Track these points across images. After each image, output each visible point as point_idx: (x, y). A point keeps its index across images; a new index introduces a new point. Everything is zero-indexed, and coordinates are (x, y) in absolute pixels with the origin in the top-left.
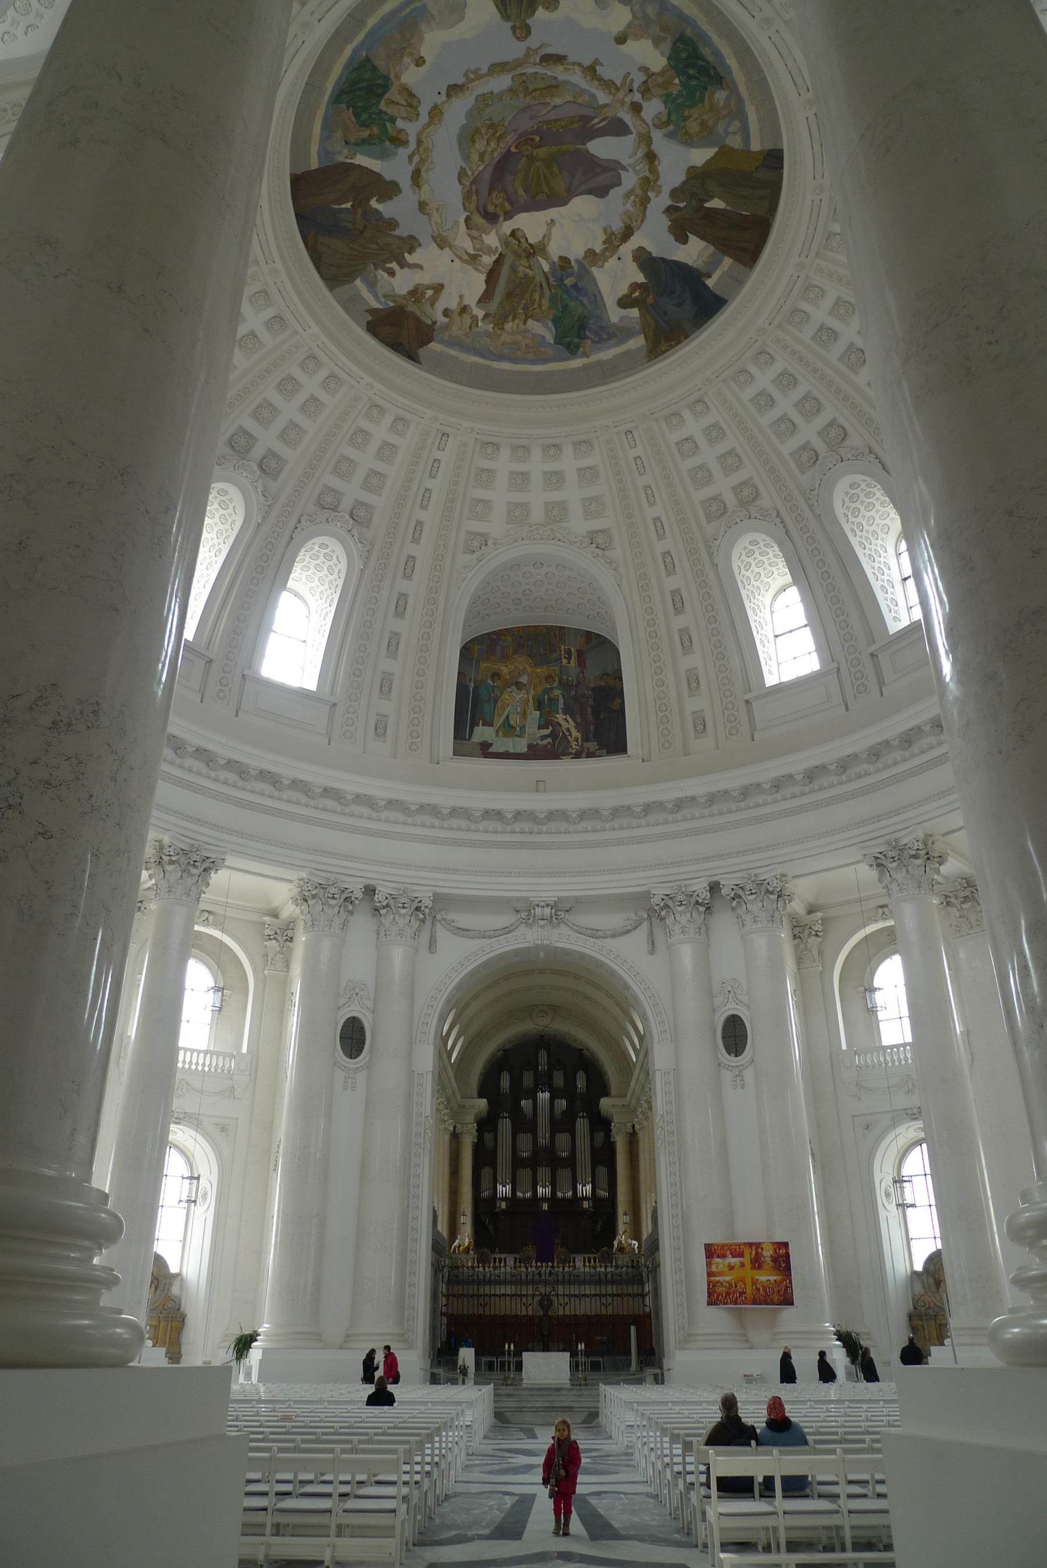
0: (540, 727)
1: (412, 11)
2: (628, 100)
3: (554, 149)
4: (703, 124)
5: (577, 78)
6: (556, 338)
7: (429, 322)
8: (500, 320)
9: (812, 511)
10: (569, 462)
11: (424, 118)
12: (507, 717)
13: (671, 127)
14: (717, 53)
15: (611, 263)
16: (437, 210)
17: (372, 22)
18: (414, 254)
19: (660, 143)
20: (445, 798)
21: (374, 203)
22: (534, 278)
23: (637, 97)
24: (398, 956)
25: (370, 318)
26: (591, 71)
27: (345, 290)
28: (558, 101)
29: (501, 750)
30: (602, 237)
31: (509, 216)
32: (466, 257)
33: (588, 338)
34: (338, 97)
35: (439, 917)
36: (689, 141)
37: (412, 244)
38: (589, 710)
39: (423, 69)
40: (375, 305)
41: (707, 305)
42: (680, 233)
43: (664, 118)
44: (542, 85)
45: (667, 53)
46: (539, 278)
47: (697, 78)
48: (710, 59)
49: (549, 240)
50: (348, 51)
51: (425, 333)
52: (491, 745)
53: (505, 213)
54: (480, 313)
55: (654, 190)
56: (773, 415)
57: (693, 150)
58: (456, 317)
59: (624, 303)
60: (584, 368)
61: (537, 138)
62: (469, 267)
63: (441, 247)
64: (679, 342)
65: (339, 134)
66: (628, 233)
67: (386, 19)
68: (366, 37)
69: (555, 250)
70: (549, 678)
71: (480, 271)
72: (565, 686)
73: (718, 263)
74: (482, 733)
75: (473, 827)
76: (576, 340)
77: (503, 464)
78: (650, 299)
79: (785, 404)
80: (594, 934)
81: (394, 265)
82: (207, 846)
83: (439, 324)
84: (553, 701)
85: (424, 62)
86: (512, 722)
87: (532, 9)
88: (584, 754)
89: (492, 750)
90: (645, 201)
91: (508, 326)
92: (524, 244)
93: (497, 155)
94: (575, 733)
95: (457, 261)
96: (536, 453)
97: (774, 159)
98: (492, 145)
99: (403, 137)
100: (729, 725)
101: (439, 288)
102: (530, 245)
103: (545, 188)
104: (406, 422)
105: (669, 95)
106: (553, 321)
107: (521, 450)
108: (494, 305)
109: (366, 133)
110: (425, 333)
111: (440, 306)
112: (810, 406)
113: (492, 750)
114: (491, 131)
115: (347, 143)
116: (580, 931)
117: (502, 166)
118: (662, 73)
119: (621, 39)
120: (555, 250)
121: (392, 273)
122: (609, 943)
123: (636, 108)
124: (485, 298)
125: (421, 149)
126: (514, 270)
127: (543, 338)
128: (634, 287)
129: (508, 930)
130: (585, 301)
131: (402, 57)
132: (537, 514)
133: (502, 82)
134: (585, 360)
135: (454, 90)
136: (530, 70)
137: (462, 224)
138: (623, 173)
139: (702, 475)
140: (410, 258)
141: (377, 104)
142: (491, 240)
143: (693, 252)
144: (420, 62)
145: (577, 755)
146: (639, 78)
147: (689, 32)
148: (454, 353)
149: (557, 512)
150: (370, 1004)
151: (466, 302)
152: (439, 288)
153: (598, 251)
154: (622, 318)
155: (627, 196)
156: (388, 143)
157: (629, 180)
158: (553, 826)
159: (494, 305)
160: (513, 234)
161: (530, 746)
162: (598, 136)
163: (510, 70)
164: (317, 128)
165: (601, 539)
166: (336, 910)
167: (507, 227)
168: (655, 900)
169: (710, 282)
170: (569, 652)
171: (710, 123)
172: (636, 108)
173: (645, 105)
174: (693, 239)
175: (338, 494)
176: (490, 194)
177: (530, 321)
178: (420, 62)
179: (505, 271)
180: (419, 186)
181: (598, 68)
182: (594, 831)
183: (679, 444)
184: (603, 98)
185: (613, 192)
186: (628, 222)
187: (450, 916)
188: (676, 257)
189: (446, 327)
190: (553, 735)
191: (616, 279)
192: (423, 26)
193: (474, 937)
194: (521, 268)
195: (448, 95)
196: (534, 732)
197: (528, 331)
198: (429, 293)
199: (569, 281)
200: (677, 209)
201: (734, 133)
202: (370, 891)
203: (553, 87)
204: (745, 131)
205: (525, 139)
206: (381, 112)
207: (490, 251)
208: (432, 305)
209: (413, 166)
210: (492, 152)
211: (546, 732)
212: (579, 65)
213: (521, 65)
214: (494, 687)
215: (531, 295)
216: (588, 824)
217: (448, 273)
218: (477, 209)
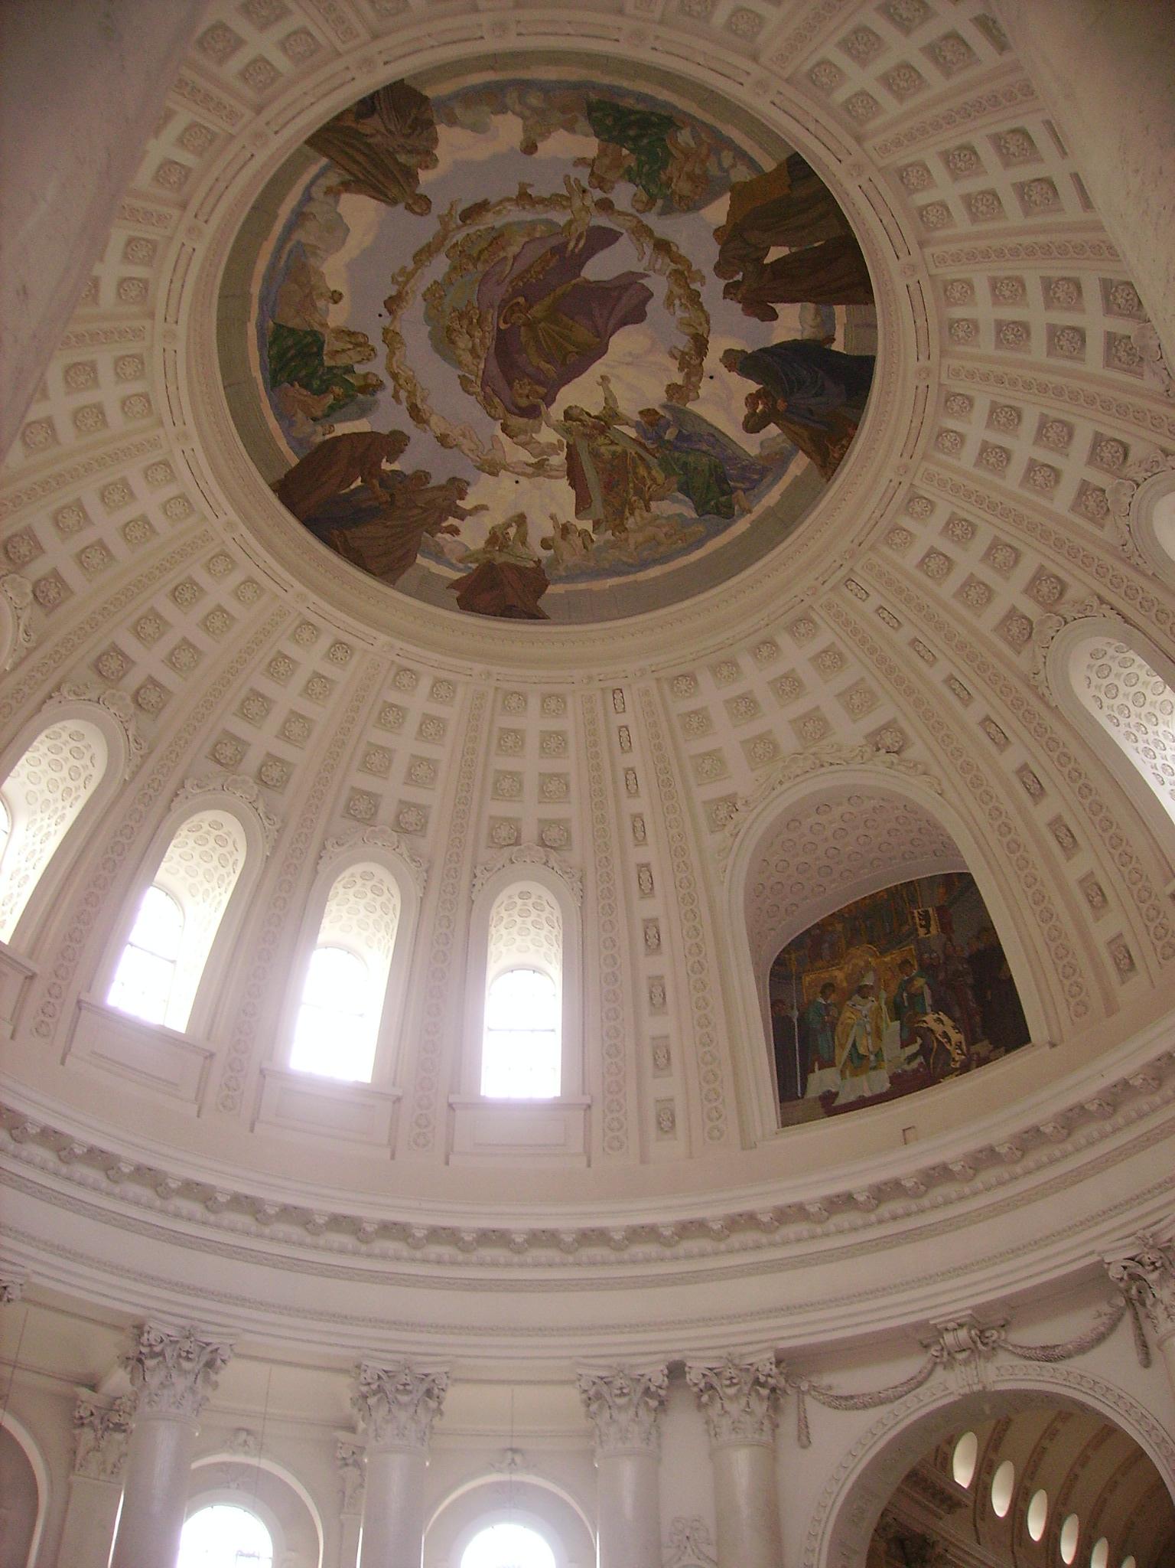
0: (903, 1045)
1: (291, 251)
2: (588, 202)
3: (548, 301)
4: (691, 177)
5: (516, 214)
7: (531, 564)
8: (616, 519)
9: (1144, 574)
10: (795, 656)
11: (382, 349)
12: (854, 1045)
13: (660, 203)
14: (641, 97)
15: (705, 388)
16: (464, 436)
17: (256, 289)
18: (467, 497)
20: (762, 1201)
21: (386, 466)
22: (625, 453)
23: (598, 194)
24: (742, 1463)
25: (457, 594)
27: (409, 576)
28: (514, 249)
29: (852, 1098)
30: (674, 365)
31: (550, 400)
32: (530, 470)
33: (736, 488)
34: (273, 382)
35: (805, 1386)
36: (691, 205)
37: (458, 487)
38: (970, 995)
39: (345, 302)
40: (456, 576)
41: (855, 376)
42: (761, 308)
43: (645, 197)
44: (484, 244)
48: (639, 107)
49: (615, 401)
50: (252, 330)
51: (535, 580)
52: (836, 1094)
54: (587, 525)
55: (694, 281)
56: (1016, 469)
57: (702, 212)
59: (753, 425)
61: (521, 300)
62: (541, 479)
63: (494, 474)
66: (701, 345)
68: (261, 308)
69: (629, 407)
70: (905, 963)
71: (557, 478)
72: (928, 969)
73: (831, 317)
74: (822, 1080)
75: (819, 1230)
76: (723, 499)
77: (711, 695)
78: (781, 405)
79: (1023, 447)
80: (1050, 1354)
81: (451, 521)
82: (419, 1358)
83: (544, 562)
84: (916, 998)
86: (862, 1051)
87: (411, 176)
88: (974, 1064)
89: (840, 1101)
90: (694, 298)
91: (630, 523)
92: (589, 421)
93: (488, 342)
94: (956, 1037)
95: (521, 479)
96: (746, 662)
98: (478, 334)
99: (372, 381)
100: (1159, 944)
101: (521, 520)
102: (596, 417)
103: (571, 348)
104: (560, 698)
105: (629, 171)
106: (680, 490)
107: (726, 667)
109: (330, 399)
110: (535, 580)
111: (534, 539)
112: (1055, 432)
113: (840, 1101)
114: (465, 322)
115: (315, 419)
116: (1027, 1354)
117: (505, 349)
118: (603, 152)
119: (530, 148)
120: (629, 407)
121: (454, 531)
122: (1078, 1364)
123: (606, 206)
124: (582, 505)
125: (401, 382)
126: (595, 455)
127: (680, 515)
128: (752, 400)
129: (917, 1382)
130: (705, 448)
131: (314, 306)
132: (788, 743)
133: (439, 266)
134: (750, 517)
135: (393, 304)
136: (459, 237)
137: (503, 437)
139: (976, 593)
140: (466, 504)
141: (322, 365)
142: (547, 435)
143: (791, 322)
144: (336, 297)
145: (965, 1068)
146: (583, 175)
147: (593, 97)
148: (582, 586)
149: (813, 725)
150: (711, 1551)
151: (562, 521)
153: (680, 382)
155: (669, 302)
157: (659, 285)
158: (938, 1193)
159: (598, 507)
161: (894, 1079)
162: (588, 258)
163: (438, 250)
164: (272, 423)
165: (888, 739)
166: (631, 1412)
167: (556, 412)
168: (1114, 1273)
169: (838, 346)
170: (926, 916)
171: (697, 171)
172: (606, 206)
173: (612, 196)
174: (778, 307)
175: (512, 822)
176: (510, 384)
179: (585, 459)
180: (426, 422)
181: (529, 191)
182: (1001, 1183)
183: (921, 564)
184: (561, 218)
185: (648, 308)
186: (692, 331)
187: (826, 1380)
188: (776, 340)
189: (556, 561)
190: (925, 1051)
191: (723, 403)
193: (865, 1407)
194: (603, 449)
195: (391, 312)
196: (897, 1054)
197: (657, 517)
198: (512, 531)
199: (670, 435)
200: (737, 284)
201: (734, 166)
202: (676, 1371)
203: (498, 238)
204: (741, 155)
205: (508, 308)
206: (331, 369)
207: (554, 449)
208: (524, 543)
209: (405, 404)
211: (914, 1048)
212: (509, 200)
213: (445, 238)
214: (826, 1006)
215: (635, 473)
216: (989, 1175)
217: (521, 498)
218: (509, 411)
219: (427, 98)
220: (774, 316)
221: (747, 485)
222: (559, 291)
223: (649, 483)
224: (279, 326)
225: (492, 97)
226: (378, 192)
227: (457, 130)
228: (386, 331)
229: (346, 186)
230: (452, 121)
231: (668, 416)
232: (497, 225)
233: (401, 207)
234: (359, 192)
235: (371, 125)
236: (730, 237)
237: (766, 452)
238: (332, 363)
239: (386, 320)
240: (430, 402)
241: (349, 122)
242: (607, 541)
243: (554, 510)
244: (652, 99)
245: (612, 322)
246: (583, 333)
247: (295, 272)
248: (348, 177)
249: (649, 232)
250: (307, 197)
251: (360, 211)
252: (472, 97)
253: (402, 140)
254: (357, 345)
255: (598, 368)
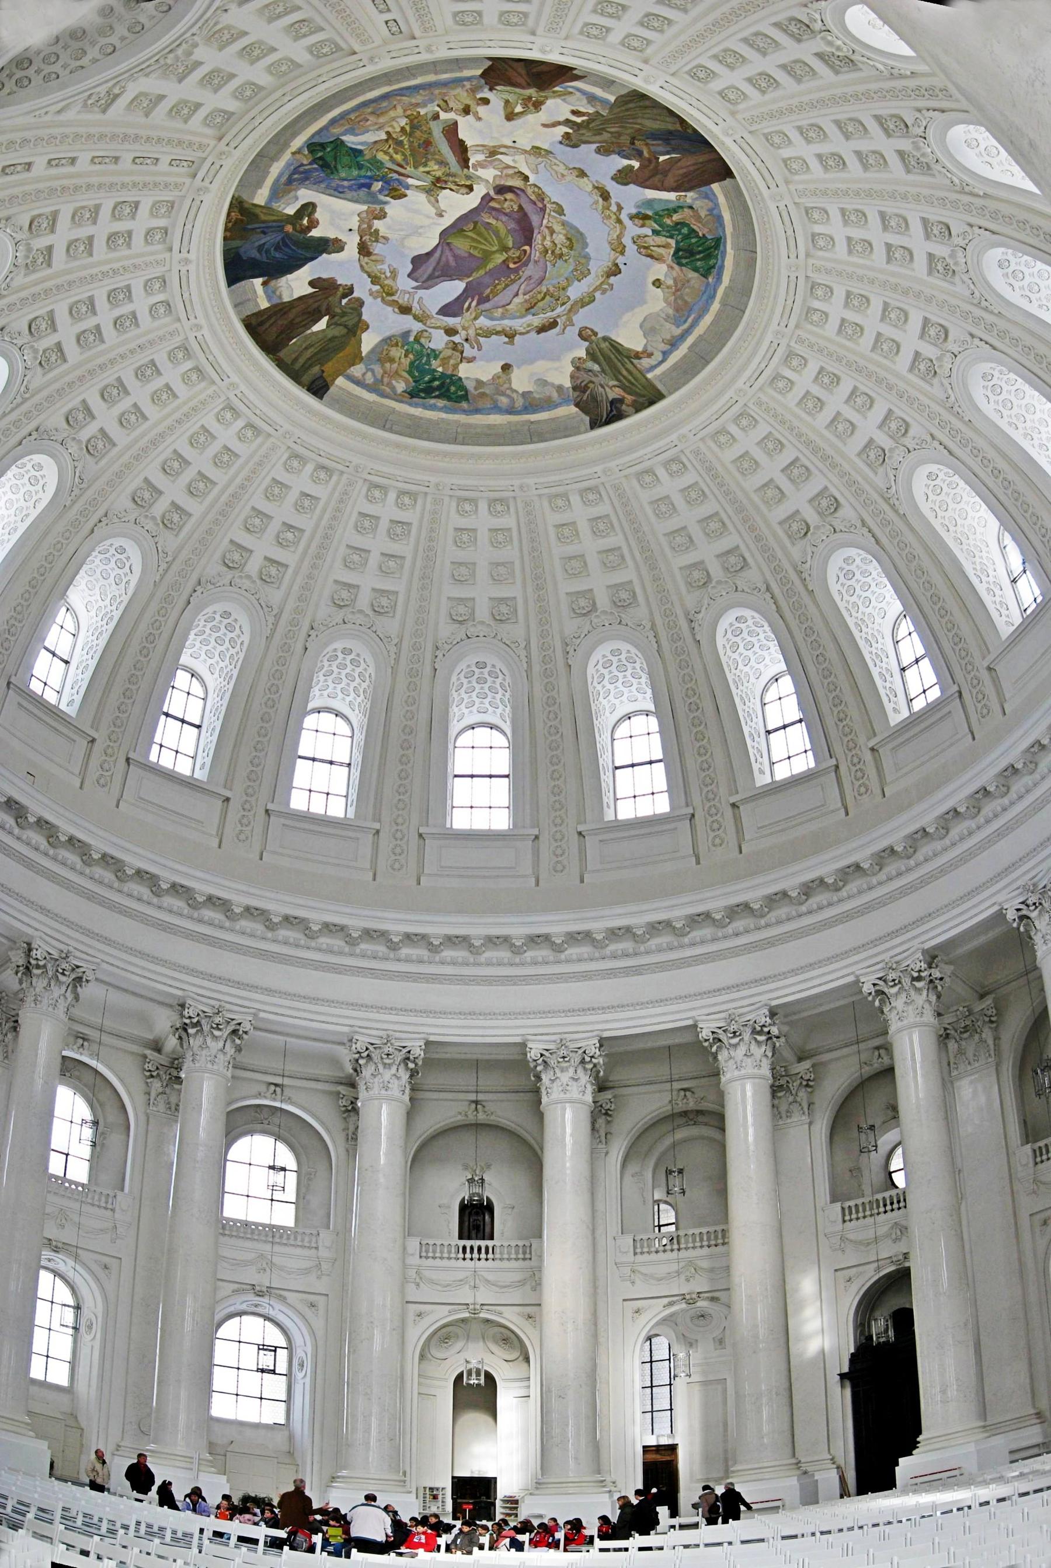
3: (490, 266)
4: (392, 360)
6: (342, 142)
11: (627, 241)
13: (412, 339)
14: (433, 408)
15: (355, 223)
17: (716, 306)
19: (408, 323)
21: (636, 164)
22: (416, 168)
23: (457, 339)
26: (511, 336)
28: (516, 300)
30: (383, 232)
31: (486, 199)
32: (502, 150)
34: (719, 242)
36: (389, 341)
41: (237, 269)
42: (324, 287)
43: (423, 341)
44: (540, 304)
45: (466, 383)
46: (409, 170)
47: (430, 381)
48: (432, 401)
53: (492, 199)
58: (468, 102)
59: (308, 209)
60: (286, 145)
61: (512, 266)
63: (533, 147)
64: (226, 230)
65: (703, 213)
66: (364, 250)
67: (705, 310)
73: (269, 298)
76: (320, 154)
78: (289, 228)
85: (654, 284)
87: (591, 355)
90: (375, 280)
91: (403, 122)
92: (450, 185)
93: (537, 238)
97: (318, 388)
98: (548, 243)
101: (510, 117)
105: (435, 358)
106: (360, 152)
108: (437, 130)
109: (676, 217)
114: (557, 252)
115: (691, 207)
117: (526, 232)
118: (456, 367)
123: (451, 332)
124: (451, 131)
126: (442, 163)
128: (314, 224)
130: (346, 183)
133: (575, 291)
135: (615, 271)
136: (559, 310)
137: (527, 172)
138: (415, 284)
141: (677, 242)
142: (489, 174)
144: (657, 283)
146: (468, 352)
147: (464, 405)
151: (470, 118)
152: (510, 117)
154: (297, 198)
156: (650, 213)
157: (404, 283)
159: (437, 130)
160: (471, 188)
163: (576, 303)
164: (727, 216)
167: (480, 191)
169: (258, 282)
171: (388, 365)
172: (451, 332)
173: (447, 338)
174: (311, 290)
176: (520, 207)
177: (384, 137)
178: (657, 283)
184: (483, 322)
185: (410, 267)
186: (373, 257)
189: (474, 91)
191: (336, 215)
192: (671, 311)
194: (436, 167)
197: (380, 128)
198: (519, 109)
199: (377, 186)
200: (344, 296)
201: (364, 374)
203: (530, 308)
205: (523, 261)
206: (671, 237)
207: (480, 165)
209: (613, 201)
210: (544, 238)
212: (521, 334)
213: (570, 311)
215: (403, 154)
219: (577, 405)
220: (312, 283)
221: (301, 169)
222: (482, 272)
223: (391, 150)
224: (705, 276)
225: (531, 405)
226: (615, 347)
227: (557, 382)
228: (622, 253)
229: (637, 356)
230: (560, 388)
231: (382, 198)
232: (530, 317)
233: (600, 335)
234: (629, 350)
235: (614, 393)
236: (355, 327)
237: (292, 194)
238: (669, 240)
239: (620, 260)
240: (589, 198)
241: (629, 398)
242: (425, 105)
243: (478, 124)
244: (425, 407)
245: (437, 255)
246: (461, 245)
247: (684, 311)
248: (635, 361)
249: (416, 318)
250: (666, 354)
251: (630, 337)
252: (547, 404)
253: (594, 379)
254: (646, 248)
255: (447, 221)
